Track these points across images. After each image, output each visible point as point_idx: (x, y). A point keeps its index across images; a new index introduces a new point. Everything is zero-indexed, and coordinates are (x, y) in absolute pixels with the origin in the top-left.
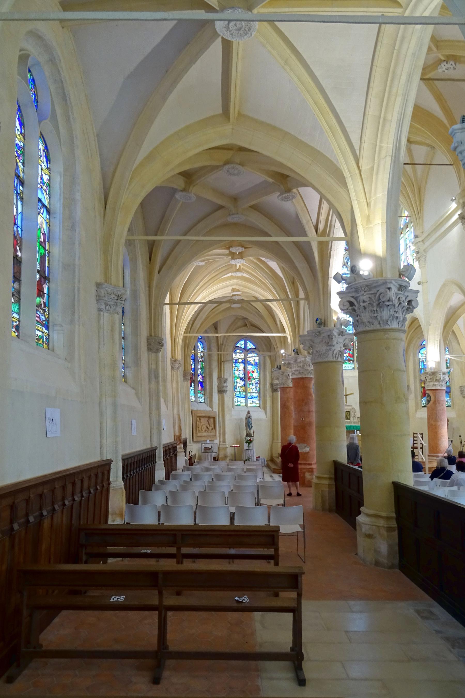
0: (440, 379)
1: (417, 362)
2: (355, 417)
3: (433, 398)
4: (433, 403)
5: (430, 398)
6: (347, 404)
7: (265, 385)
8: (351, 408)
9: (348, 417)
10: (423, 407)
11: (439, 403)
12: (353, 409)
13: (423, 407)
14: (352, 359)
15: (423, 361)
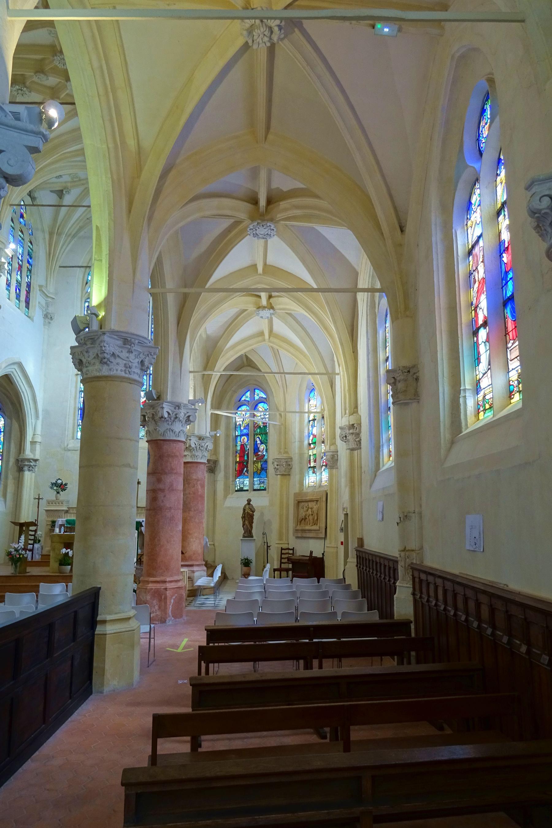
1: (233, 426)
7: (8, 461)
10: (236, 491)
13: (236, 491)
15: (240, 425)
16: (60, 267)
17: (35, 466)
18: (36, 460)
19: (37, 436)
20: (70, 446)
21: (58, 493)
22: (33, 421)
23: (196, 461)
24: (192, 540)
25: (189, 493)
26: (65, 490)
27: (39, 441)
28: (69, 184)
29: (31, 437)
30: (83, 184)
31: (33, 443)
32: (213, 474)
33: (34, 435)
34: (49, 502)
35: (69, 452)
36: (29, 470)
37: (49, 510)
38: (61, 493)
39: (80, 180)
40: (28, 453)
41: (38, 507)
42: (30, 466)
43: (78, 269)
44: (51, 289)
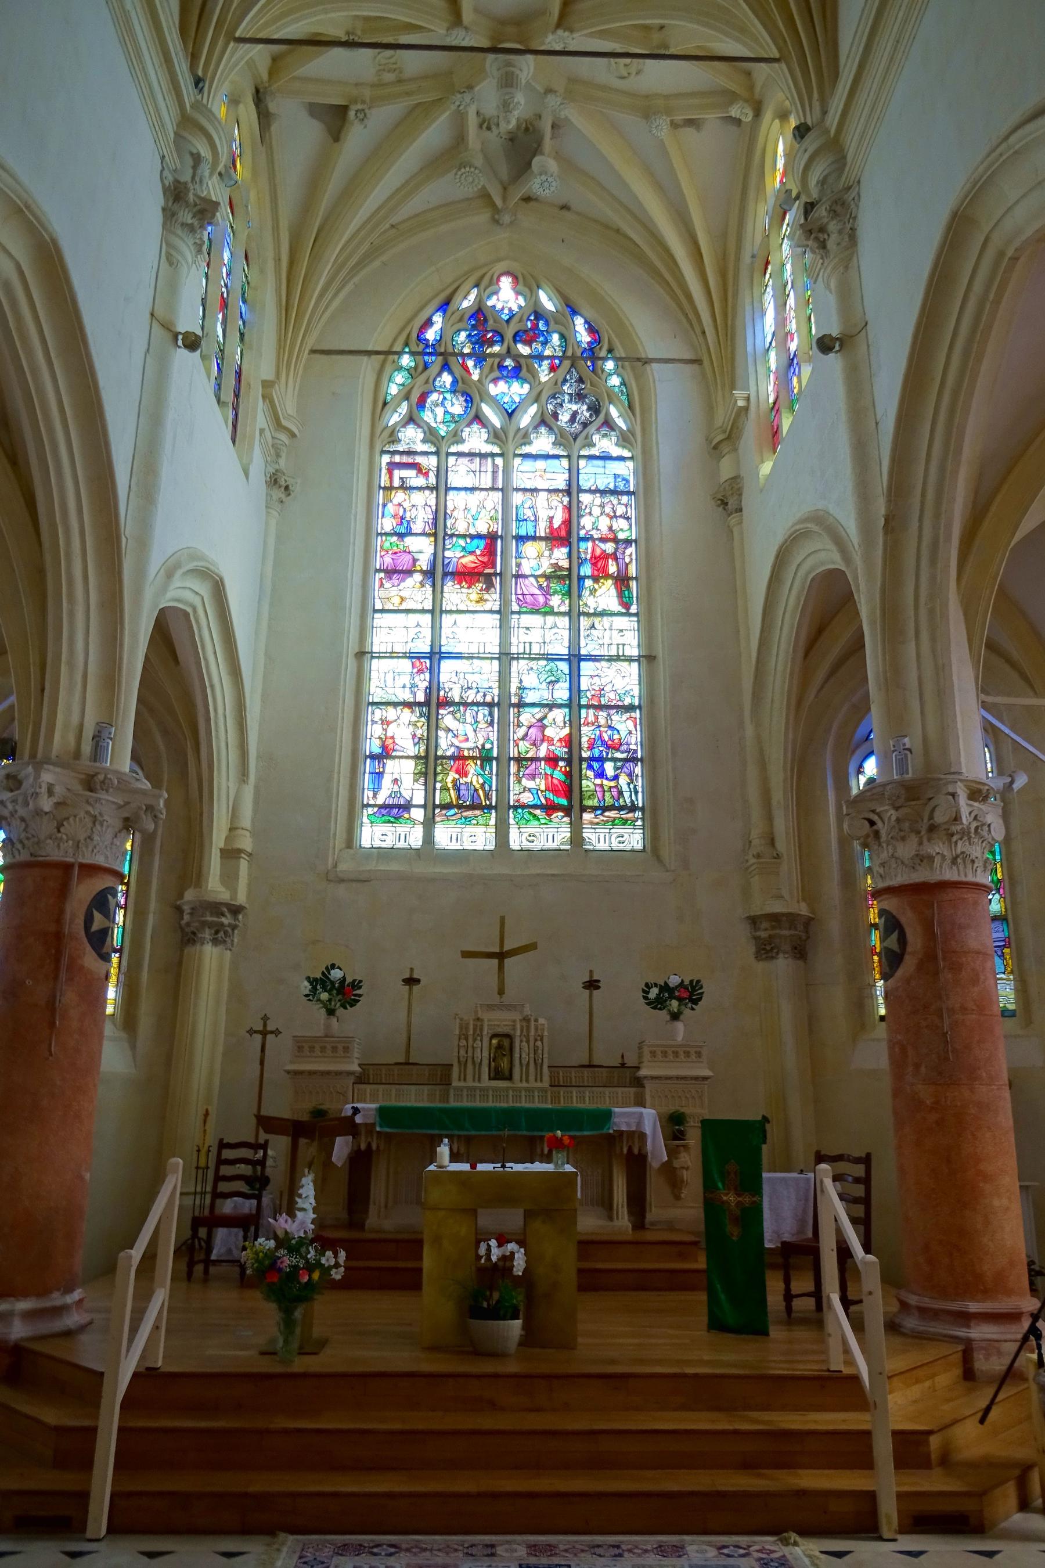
0: (957, 818)
2: (538, 1066)
3: (915, 940)
4: (920, 967)
5: (902, 941)
6: (506, 999)
8: (517, 1016)
9: (504, 1064)
11: (956, 968)
12: (526, 1020)
14: (564, 802)
16: (313, 352)
17: (234, 927)
18: (236, 910)
19: (240, 832)
20: (342, 867)
21: (331, 1012)
22: (231, 785)
23: (970, 878)
24: (996, 1203)
25: (964, 1009)
26: (353, 1003)
27: (249, 850)
28: (367, 93)
29: (224, 834)
30: (408, 94)
31: (231, 854)
32: (800, 963)
33: (231, 829)
34: (303, 1046)
35: (342, 886)
36: (215, 942)
37: (301, 1073)
38: (340, 1011)
39: (400, 81)
40: (215, 887)
41: (262, 1063)
42: (218, 928)
43: (365, 358)
44: (288, 403)
